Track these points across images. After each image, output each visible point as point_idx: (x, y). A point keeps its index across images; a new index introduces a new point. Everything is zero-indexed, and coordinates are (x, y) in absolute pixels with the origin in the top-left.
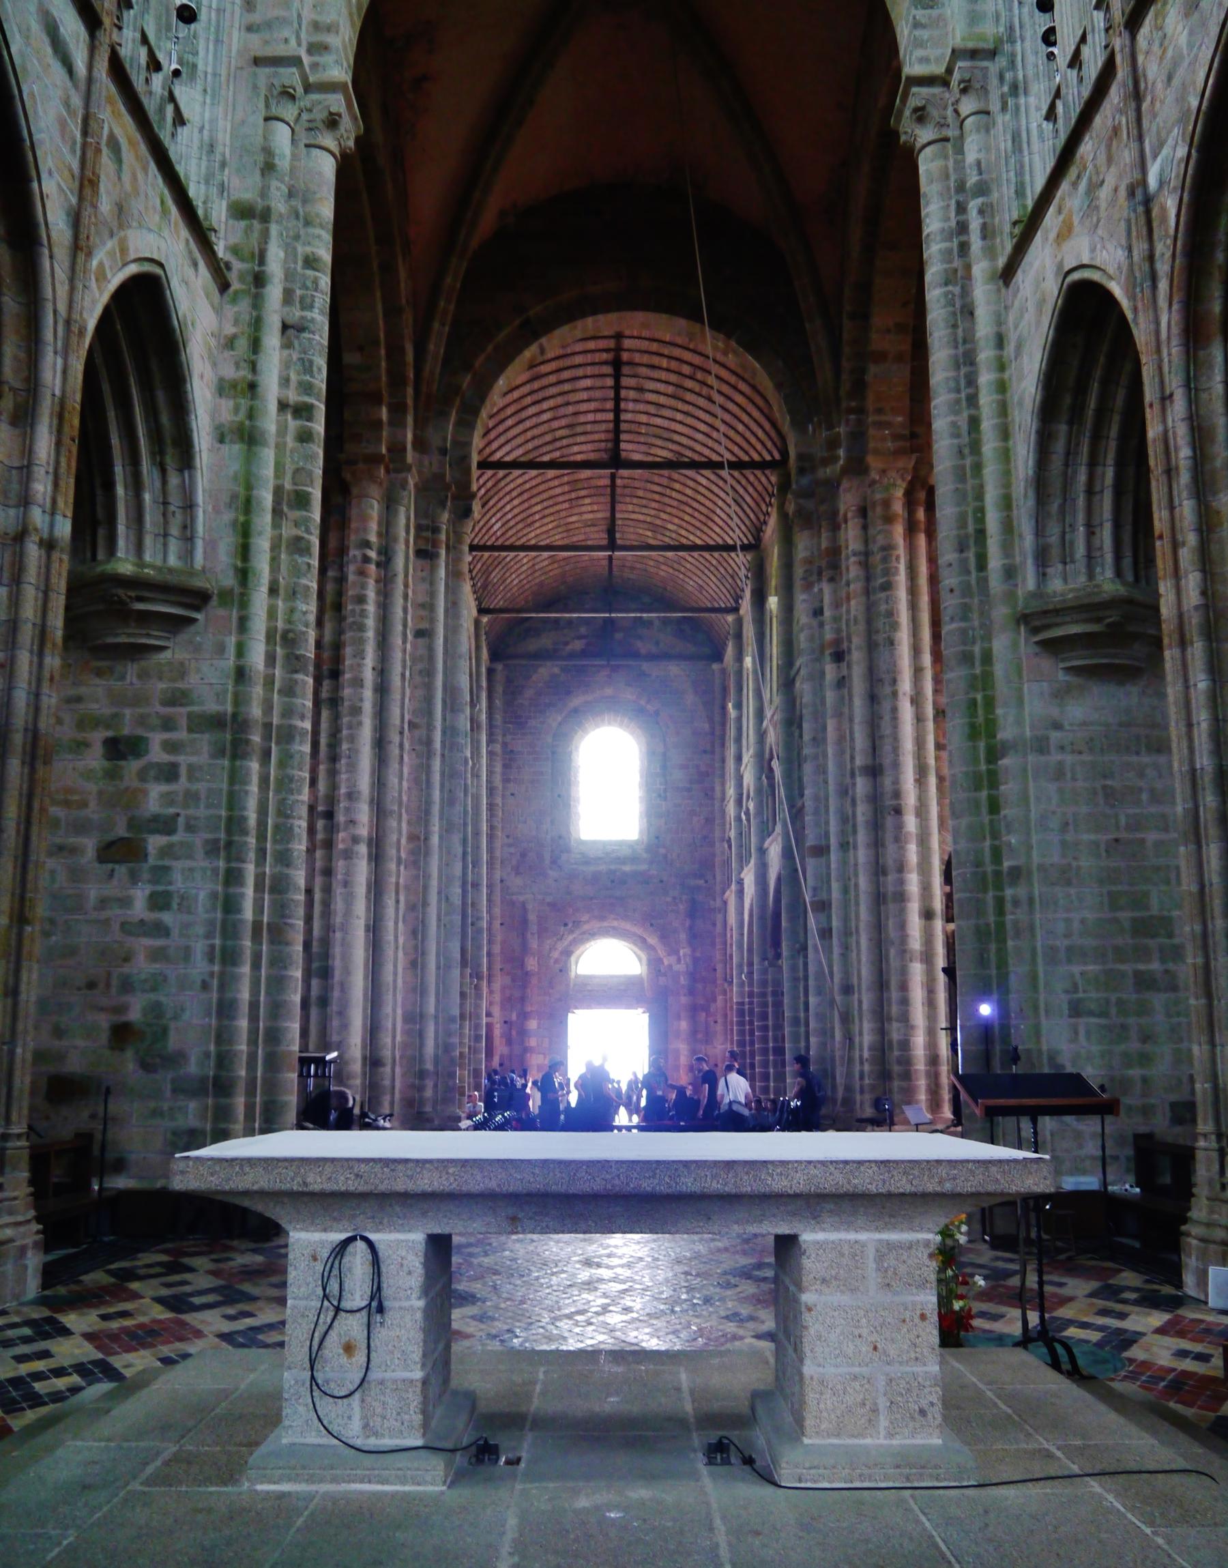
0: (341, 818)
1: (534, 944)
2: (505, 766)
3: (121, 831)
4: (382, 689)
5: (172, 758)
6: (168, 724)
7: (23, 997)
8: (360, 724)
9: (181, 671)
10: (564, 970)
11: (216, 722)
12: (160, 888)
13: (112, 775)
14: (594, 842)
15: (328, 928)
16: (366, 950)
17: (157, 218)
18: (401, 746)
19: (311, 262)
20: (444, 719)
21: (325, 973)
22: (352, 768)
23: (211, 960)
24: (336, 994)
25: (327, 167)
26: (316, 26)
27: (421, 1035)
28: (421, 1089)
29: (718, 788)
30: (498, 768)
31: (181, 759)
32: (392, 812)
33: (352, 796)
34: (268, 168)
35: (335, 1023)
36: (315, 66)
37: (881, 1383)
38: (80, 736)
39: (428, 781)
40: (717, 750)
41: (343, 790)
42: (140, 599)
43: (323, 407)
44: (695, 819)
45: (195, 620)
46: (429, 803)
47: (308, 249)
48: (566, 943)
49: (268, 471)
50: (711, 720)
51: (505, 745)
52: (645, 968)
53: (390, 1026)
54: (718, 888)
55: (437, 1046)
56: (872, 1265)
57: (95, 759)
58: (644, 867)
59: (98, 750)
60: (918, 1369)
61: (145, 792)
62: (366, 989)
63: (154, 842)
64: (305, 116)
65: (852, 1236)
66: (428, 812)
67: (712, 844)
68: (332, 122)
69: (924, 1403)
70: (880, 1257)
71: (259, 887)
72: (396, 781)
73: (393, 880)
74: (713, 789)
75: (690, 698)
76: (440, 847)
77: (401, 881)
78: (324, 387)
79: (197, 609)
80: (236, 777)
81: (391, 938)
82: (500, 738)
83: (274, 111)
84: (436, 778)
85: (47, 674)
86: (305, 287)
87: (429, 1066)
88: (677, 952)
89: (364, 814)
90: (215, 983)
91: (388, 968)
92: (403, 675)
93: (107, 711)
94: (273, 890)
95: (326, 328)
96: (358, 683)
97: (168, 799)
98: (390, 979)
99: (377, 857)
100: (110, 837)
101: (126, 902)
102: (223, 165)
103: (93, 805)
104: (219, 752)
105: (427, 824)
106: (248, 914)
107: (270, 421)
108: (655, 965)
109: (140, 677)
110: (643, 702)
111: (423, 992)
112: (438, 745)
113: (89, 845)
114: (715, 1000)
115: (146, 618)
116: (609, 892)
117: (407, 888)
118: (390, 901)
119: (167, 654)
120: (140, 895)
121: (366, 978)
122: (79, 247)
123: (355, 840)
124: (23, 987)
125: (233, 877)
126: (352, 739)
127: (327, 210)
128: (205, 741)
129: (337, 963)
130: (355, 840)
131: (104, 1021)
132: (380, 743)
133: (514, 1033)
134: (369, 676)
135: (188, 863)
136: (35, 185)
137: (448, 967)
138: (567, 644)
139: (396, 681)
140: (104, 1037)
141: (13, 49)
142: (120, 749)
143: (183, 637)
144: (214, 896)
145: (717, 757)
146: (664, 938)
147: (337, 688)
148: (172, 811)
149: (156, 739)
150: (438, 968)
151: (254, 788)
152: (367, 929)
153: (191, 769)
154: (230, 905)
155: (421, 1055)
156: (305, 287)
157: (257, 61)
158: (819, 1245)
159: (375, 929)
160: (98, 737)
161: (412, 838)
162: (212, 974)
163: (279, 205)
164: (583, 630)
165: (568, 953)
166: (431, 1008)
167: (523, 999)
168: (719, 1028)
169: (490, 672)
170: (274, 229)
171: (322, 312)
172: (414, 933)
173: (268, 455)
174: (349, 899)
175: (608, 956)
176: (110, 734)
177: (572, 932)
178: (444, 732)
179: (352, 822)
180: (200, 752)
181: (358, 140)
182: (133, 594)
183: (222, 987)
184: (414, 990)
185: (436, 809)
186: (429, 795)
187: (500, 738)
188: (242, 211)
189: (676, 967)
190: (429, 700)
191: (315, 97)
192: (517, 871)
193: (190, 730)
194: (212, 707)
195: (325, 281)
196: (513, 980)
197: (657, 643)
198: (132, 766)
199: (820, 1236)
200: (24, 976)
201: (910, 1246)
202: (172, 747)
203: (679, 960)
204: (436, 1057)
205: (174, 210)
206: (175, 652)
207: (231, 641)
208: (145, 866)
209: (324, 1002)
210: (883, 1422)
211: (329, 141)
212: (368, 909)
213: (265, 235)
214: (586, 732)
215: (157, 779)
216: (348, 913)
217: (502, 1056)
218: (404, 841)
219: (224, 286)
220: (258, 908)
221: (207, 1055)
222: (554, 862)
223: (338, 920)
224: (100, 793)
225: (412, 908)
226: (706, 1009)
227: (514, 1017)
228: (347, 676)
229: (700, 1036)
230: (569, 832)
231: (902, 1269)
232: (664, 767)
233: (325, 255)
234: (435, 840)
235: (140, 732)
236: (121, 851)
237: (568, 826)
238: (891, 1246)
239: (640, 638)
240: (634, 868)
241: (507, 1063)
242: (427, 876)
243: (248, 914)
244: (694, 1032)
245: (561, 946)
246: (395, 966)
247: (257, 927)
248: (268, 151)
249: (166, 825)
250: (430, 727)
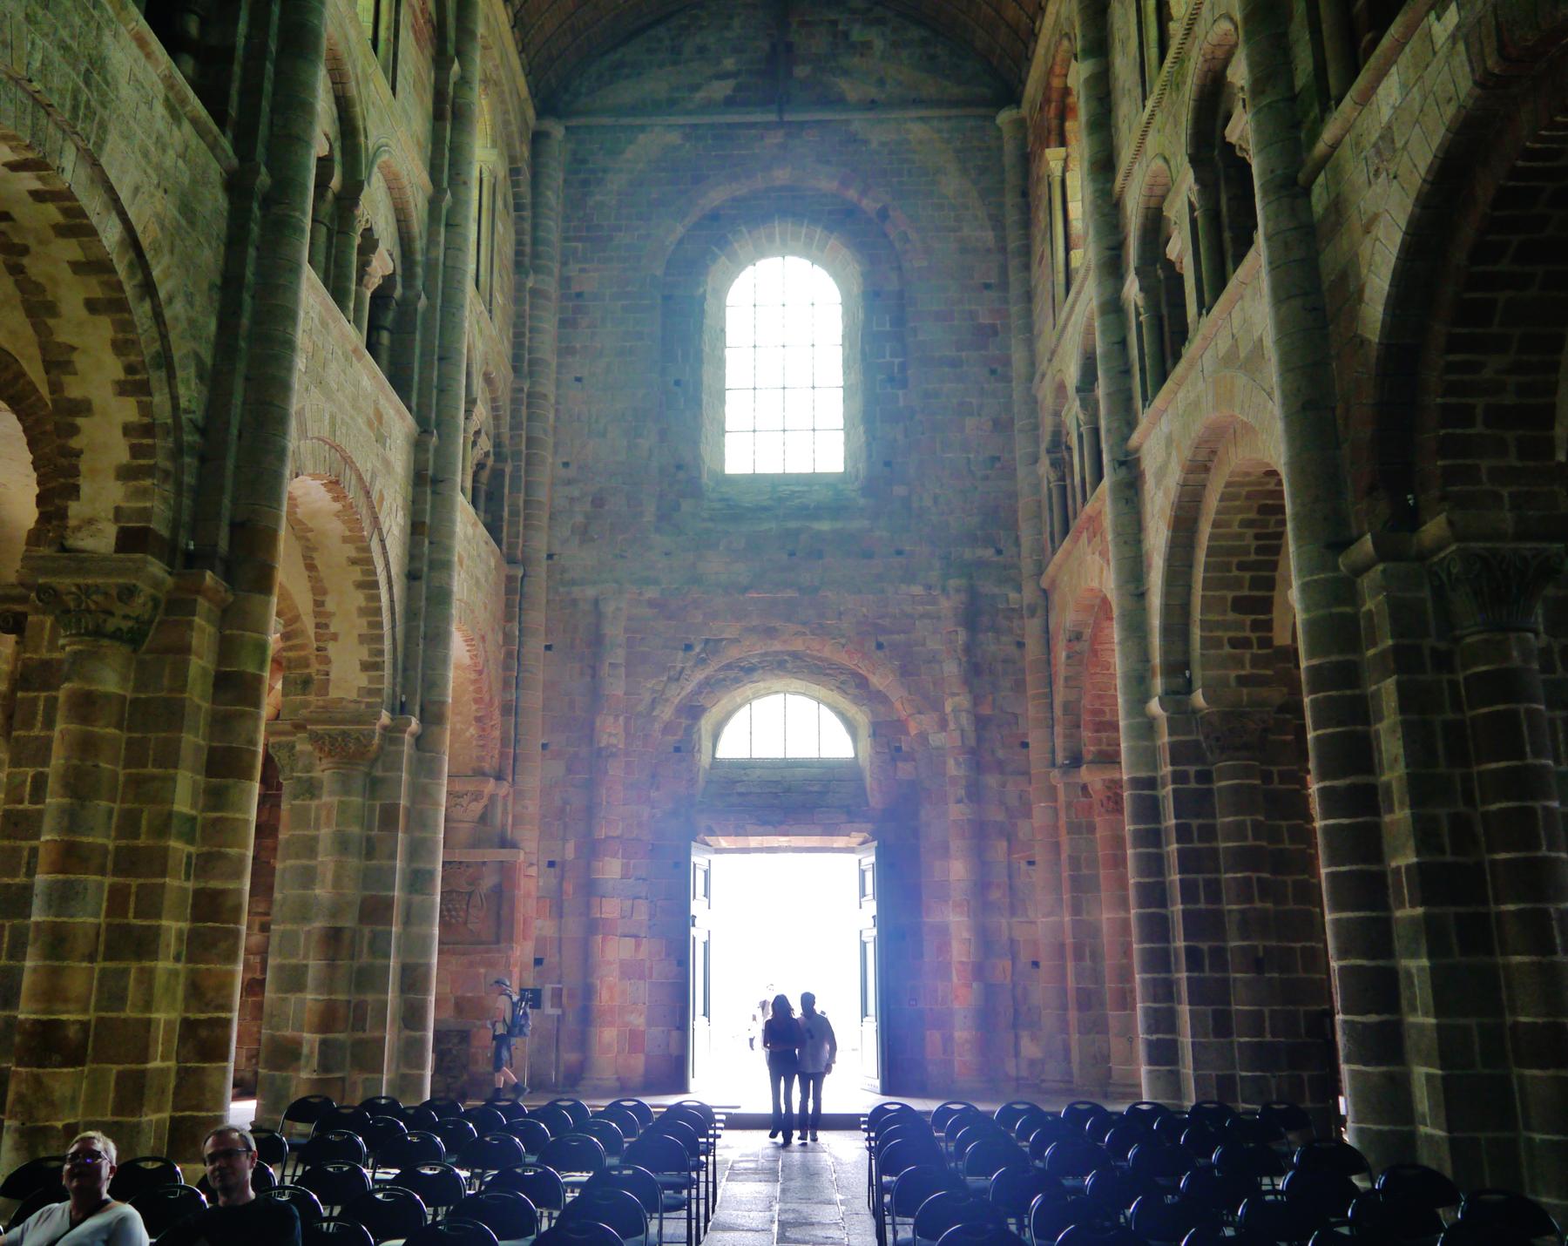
1: (616, 687)
2: (563, 323)
10: (685, 748)
14: (754, 480)
29: (1018, 356)
30: (549, 324)
40: (1013, 277)
44: (970, 422)
48: (690, 687)
50: (998, 223)
51: (565, 281)
52: (866, 743)
54: (1027, 566)
58: (856, 525)
67: (1010, 473)
74: (1007, 362)
75: (952, 184)
82: (555, 267)
88: (937, 706)
108: (887, 736)
110: (852, 194)
114: (1028, 814)
116: (792, 575)
133: (569, 887)
138: (695, 88)
145: (1015, 290)
146: (906, 672)
164: (729, 63)
165: (693, 711)
167: (590, 812)
168: (1039, 875)
169: (538, 139)
175: (786, 724)
177: (701, 662)
187: (555, 267)
189: (937, 739)
192: (584, 534)
196: (569, 770)
197: (881, 82)
203: (943, 725)
214: (741, 267)
217: (541, 942)
226: (1010, 836)
227: (570, 854)
229: (995, 895)
230: (697, 458)
232: (899, 321)
237: (695, 443)
239: (846, 73)
240: (839, 525)
241: (551, 959)
244: (981, 886)
245: (678, 694)
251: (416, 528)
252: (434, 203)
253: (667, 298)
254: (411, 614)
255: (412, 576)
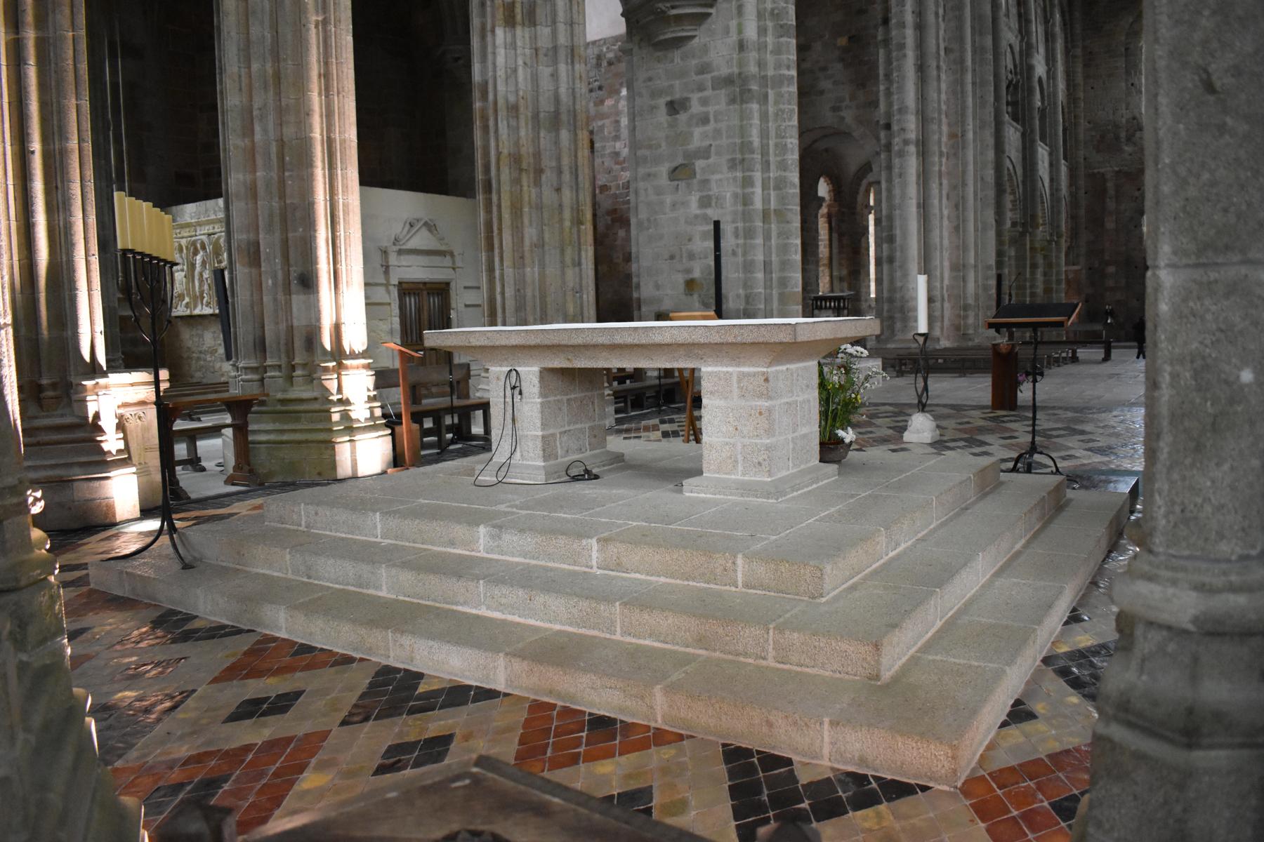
0: (895, 128)
2: (1086, 66)
3: (680, 161)
4: (920, 27)
5: (704, 109)
6: (701, 88)
7: (584, 266)
8: (905, 56)
9: (705, 49)
11: (728, 81)
12: (705, 194)
13: (672, 126)
15: (891, 207)
16: (919, 222)
18: (938, 67)
20: (973, 42)
21: (891, 239)
22: (901, 89)
23: (737, 237)
24: (898, 254)
27: (964, 280)
28: (966, 317)
30: (1079, 69)
31: (711, 109)
32: (933, 119)
33: (903, 110)
35: (898, 274)
37: (739, 447)
38: (653, 103)
39: (962, 92)
41: (896, 107)
42: (673, 7)
45: (709, 15)
46: (964, 108)
53: (938, 273)
55: (977, 287)
56: (735, 385)
57: (662, 116)
59: (663, 110)
60: (758, 441)
61: (691, 134)
62: (919, 249)
63: (699, 164)
65: (725, 369)
66: (963, 115)
69: (761, 459)
70: (739, 381)
71: (765, 187)
72: (935, 95)
73: (936, 168)
76: (974, 140)
77: (943, 168)
79: (711, 6)
80: (744, 116)
81: (936, 211)
84: (969, 87)
85: (577, 75)
87: (971, 301)
89: (911, 123)
90: (740, 251)
91: (935, 234)
92: (937, 14)
93: (666, 84)
94: (777, 188)
96: (902, 25)
97: (705, 136)
98: (937, 240)
99: (923, 154)
100: (675, 164)
101: (685, 204)
103: (663, 144)
104: (732, 101)
105: (963, 123)
106: (758, 205)
109: (682, 59)
111: (965, 249)
112: (969, 63)
113: (664, 169)
115: (679, 19)
117: (948, 174)
118: (934, 186)
119: (696, 40)
120: (694, 199)
121: (919, 241)
123: (906, 142)
124: (583, 261)
125: (748, 182)
126: (899, 68)
128: (723, 94)
129: (898, 232)
130: (906, 142)
131: (680, 279)
132: (921, 68)
134: (909, 18)
135: (718, 176)
137: (984, 229)
139: (931, 18)
140: (682, 287)
142: (674, 107)
143: (704, 27)
144: (735, 196)
147: (887, 31)
148: (708, 143)
149: (695, 97)
150: (976, 230)
151: (756, 121)
152: (918, 206)
153: (717, 114)
154: (746, 201)
155: (965, 293)
158: (710, 373)
159: (924, 206)
160: (662, 102)
161: (952, 136)
162: (738, 245)
166: (972, 261)
172: (957, 206)
174: (904, 186)
176: (669, 99)
178: (974, 52)
179: (903, 130)
180: (719, 102)
182: (668, 5)
183: (745, 254)
184: (958, 247)
185: (970, 112)
186: (964, 102)
190: (960, 28)
193: (713, 89)
194: (724, 71)
198: (682, 117)
199: (709, 369)
200: (583, 254)
201: (754, 375)
202: (704, 102)
204: (977, 296)
206: (701, 38)
207: (733, 24)
208: (695, 181)
209: (891, 260)
210: (740, 468)
212: (918, 191)
215: (697, 125)
216: (904, 196)
218: (944, 139)
220: (766, 200)
221: (738, 296)
222: (1129, 139)
223: (897, 201)
224: (667, 137)
225: (954, 187)
228: (894, 21)
231: (751, 387)
234: (970, 135)
235: (685, 95)
236: (681, 172)
238: (745, 375)
242: (965, 165)
243: (758, 205)
246: (941, 232)
247: (766, 215)
249: (705, 153)
250: (962, 50)
251: (1052, 180)
252: (1048, 72)
253: (1127, 49)
254: (1052, 207)
255: (1052, 195)
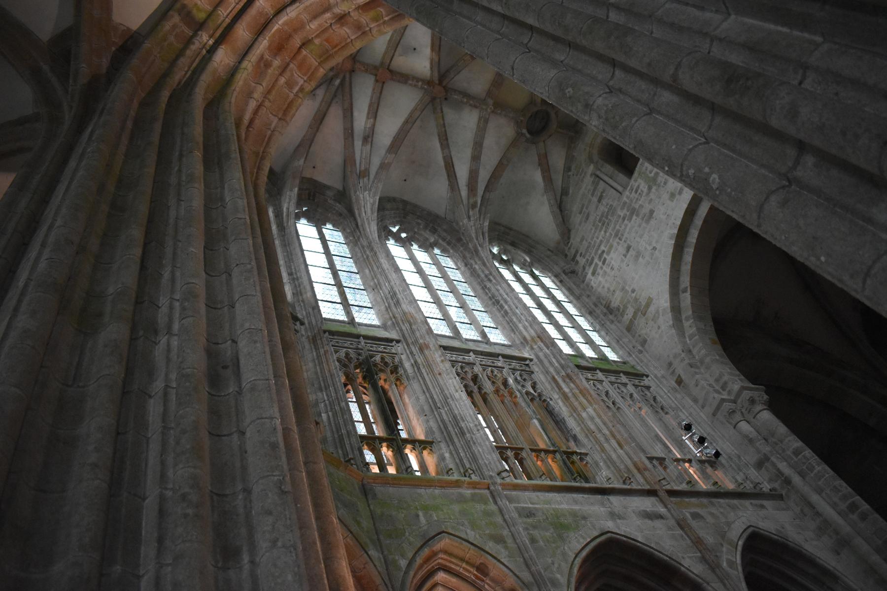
17: (732, 514)
19: (797, 452)
25: (766, 416)
26: (717, 380)
34: (751, 441)
36: (729, 393)
43: (858, 497)
47: (791, 449)
49: (865, 547)
64: (743, 410)
68: (752, 401)
78: (850, 489)
83: (734, 423)
86: (804, 463)
95: (827, 468)
102: (739, 457)
107: (846, 529)
122: (714, 567)
127: (782, 429)
136: (682, 568)
141: (639, 540)
156: (804, 463)
157: (714, 415)
163: (767, 449)
170: (773, 459)
171: (818, 465)
173: (859, 541)
181: (766, 393)
188: (759, 465)
191: (739, 401)
195: (808, 452)
205: (735, 502)
211: (759, 407)
213: (774, 465)
219: (780, 497)
233: (798, 444)
248: (746, 436)
